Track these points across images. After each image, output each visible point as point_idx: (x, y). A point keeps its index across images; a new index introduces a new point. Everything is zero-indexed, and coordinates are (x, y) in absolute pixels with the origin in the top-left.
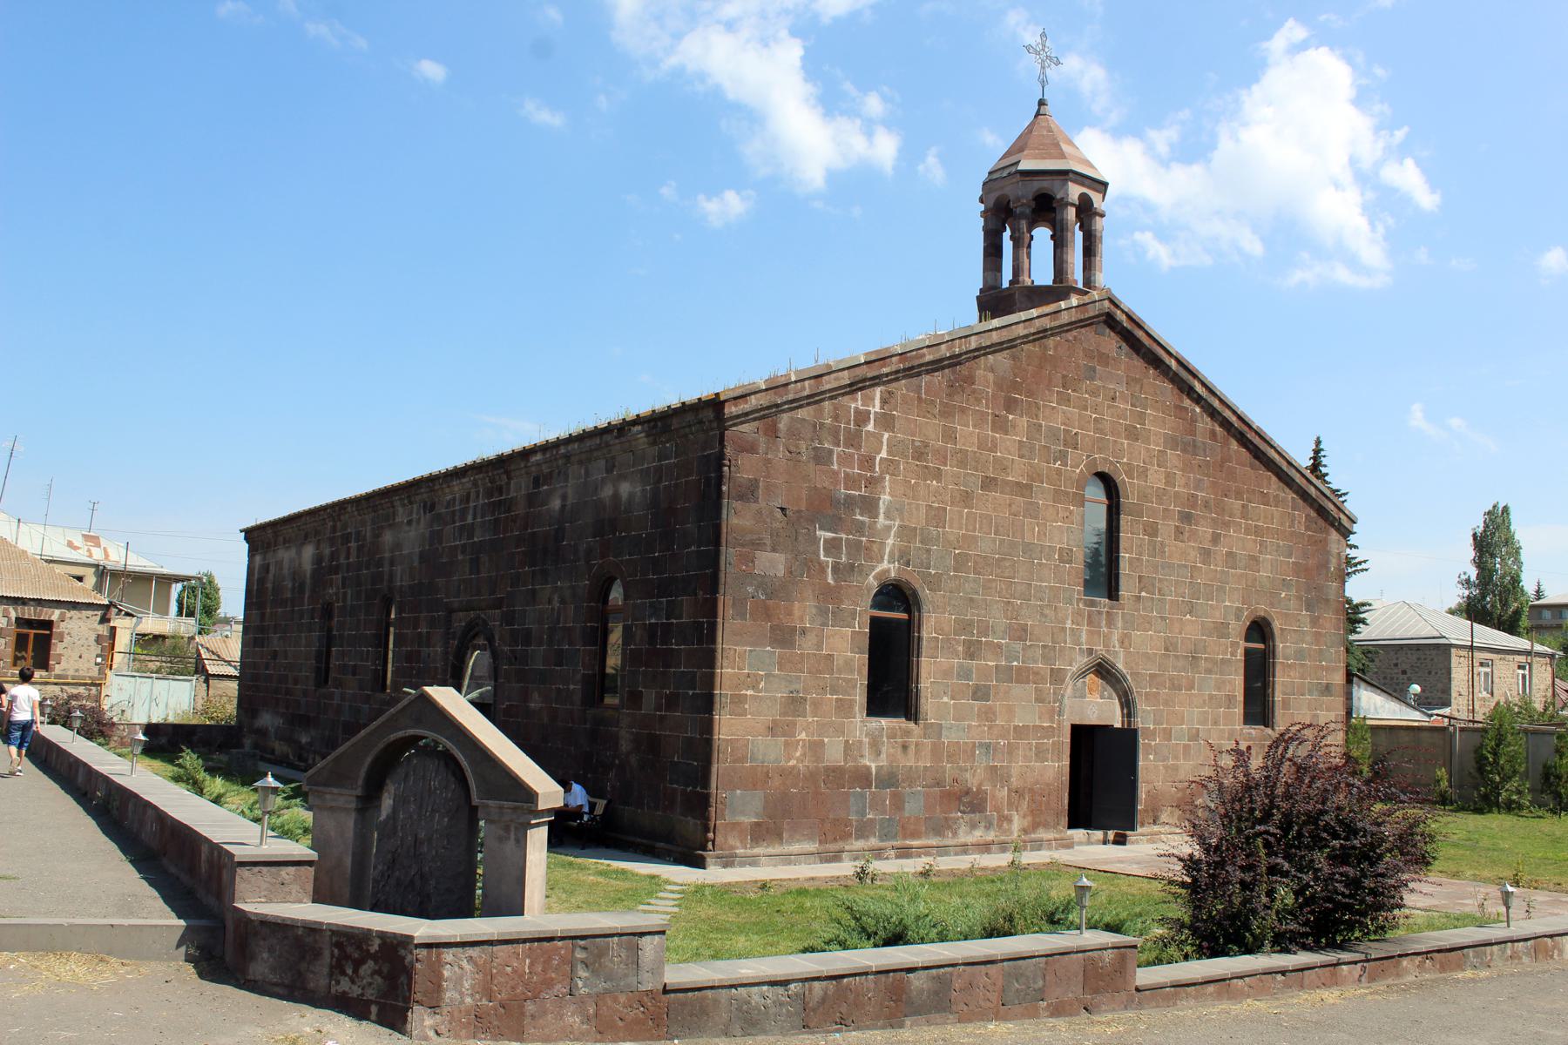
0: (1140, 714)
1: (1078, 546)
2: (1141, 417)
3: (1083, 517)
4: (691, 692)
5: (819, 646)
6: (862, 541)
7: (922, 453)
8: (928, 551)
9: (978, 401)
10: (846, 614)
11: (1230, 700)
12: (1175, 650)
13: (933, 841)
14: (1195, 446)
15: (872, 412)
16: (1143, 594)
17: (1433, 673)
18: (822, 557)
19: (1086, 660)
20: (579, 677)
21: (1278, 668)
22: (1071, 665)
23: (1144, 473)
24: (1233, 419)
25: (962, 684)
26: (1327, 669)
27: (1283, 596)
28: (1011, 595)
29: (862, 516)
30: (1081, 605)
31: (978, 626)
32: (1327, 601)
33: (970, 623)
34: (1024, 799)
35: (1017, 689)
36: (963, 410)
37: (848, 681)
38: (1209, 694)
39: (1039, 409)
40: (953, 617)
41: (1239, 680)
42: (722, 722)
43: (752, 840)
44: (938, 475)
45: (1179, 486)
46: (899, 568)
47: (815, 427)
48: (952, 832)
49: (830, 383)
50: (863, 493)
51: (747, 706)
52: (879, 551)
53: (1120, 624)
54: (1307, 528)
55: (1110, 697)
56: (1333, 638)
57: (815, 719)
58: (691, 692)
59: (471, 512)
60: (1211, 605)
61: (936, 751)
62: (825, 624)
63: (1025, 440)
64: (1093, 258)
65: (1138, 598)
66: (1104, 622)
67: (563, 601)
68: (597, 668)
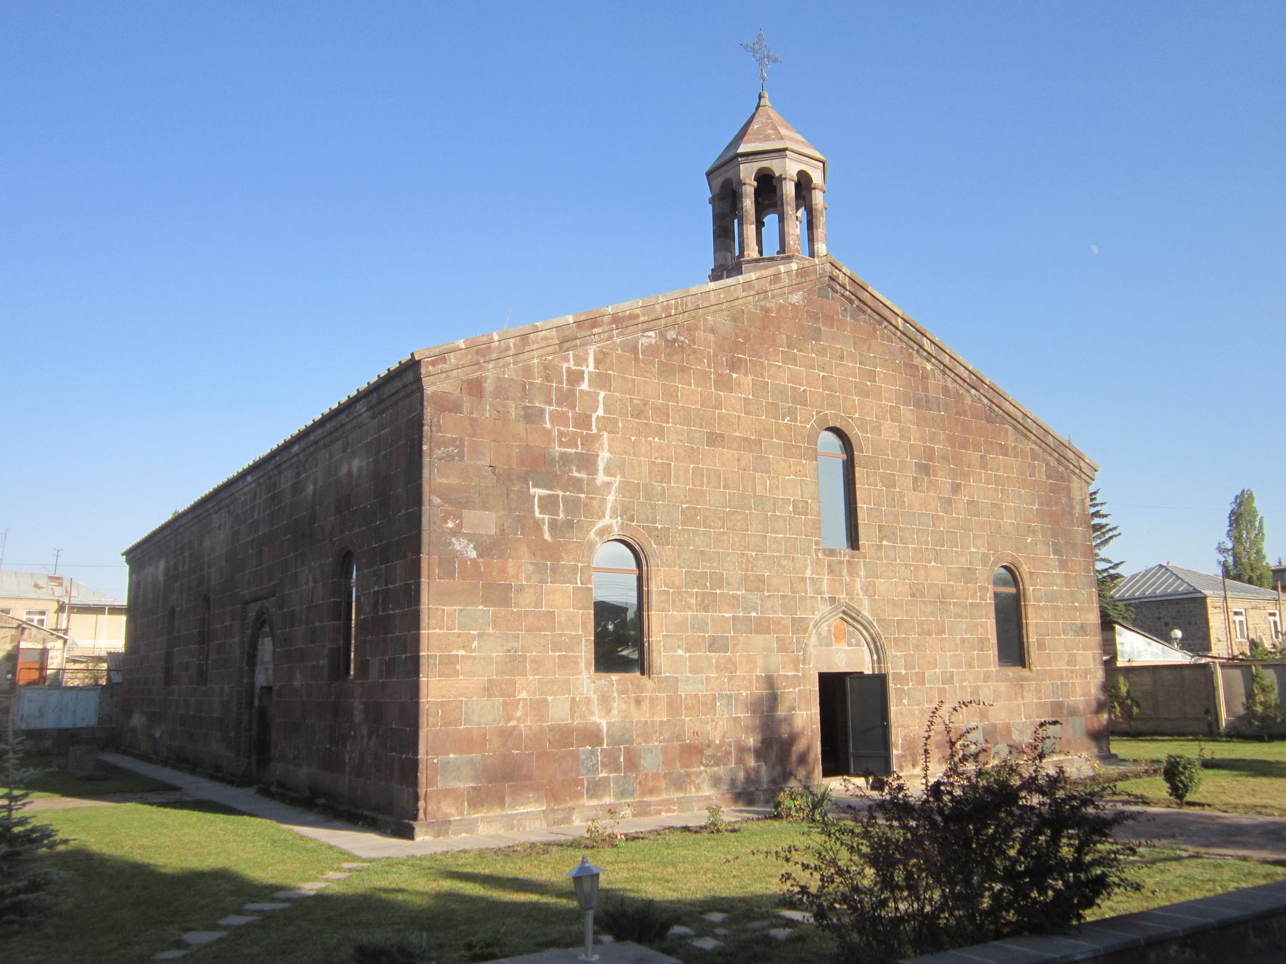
0: (889, 659)
1: (813, 499)
2: (872, 375)
3: (816, 469)
4: (403, 656)
5: (538, 603)
6: (580, 498)
7: (642, 411)
8: (654, 507)
9: (700, 361)
10: (566, 571)
11: (983, 643)
12: (923, 595)
13: (676, 795)
14: (927, 401)
15: (586, 372)
16: (885, 543)
17: (1193, 623)
18: (537, 514)
19: (829, 608)
20: (326, 651)
21: (1030, 610)
22: (813, 614)
23: (877, 429)
24: (965, 374)
25: (699, 636)
26: (1080, 609)
27: (1029, 540)
28: (745, 548)
29: (579, 471)
30: (820, 555)
31: (711, 579)
32: (1074, 544)
33: (704, 575)
34: (772, 748)
35: (757, 639)
36: (684, 370)
37: (572, 638)
38: (961, 638)
39: (764, 367)
40: (684, 570)
41: (991, 624)
42: (431, 684)
43: (469, 805)
44: (660, 433)
45: (915, 439)
46: (623, 523)
47: (524, 386)
48: (696, 788)
49: (536, 342)
50: (579, 451)
51: (458, 667)
52: (600, 507)
53: (862, 573)
54: (1048, 477)
55: (858, 644)
56: (1084, 580)
57: (537, 677)
58: (403, 656)
59: (257, 509)
60: (956, 552)
61: (674, 706)
62: (543, 581)
63: (751, 397)
64: (814, 231)
65: (880, 547)
66: (846, 571)
67: (315, 581)
68: (341, 642)
